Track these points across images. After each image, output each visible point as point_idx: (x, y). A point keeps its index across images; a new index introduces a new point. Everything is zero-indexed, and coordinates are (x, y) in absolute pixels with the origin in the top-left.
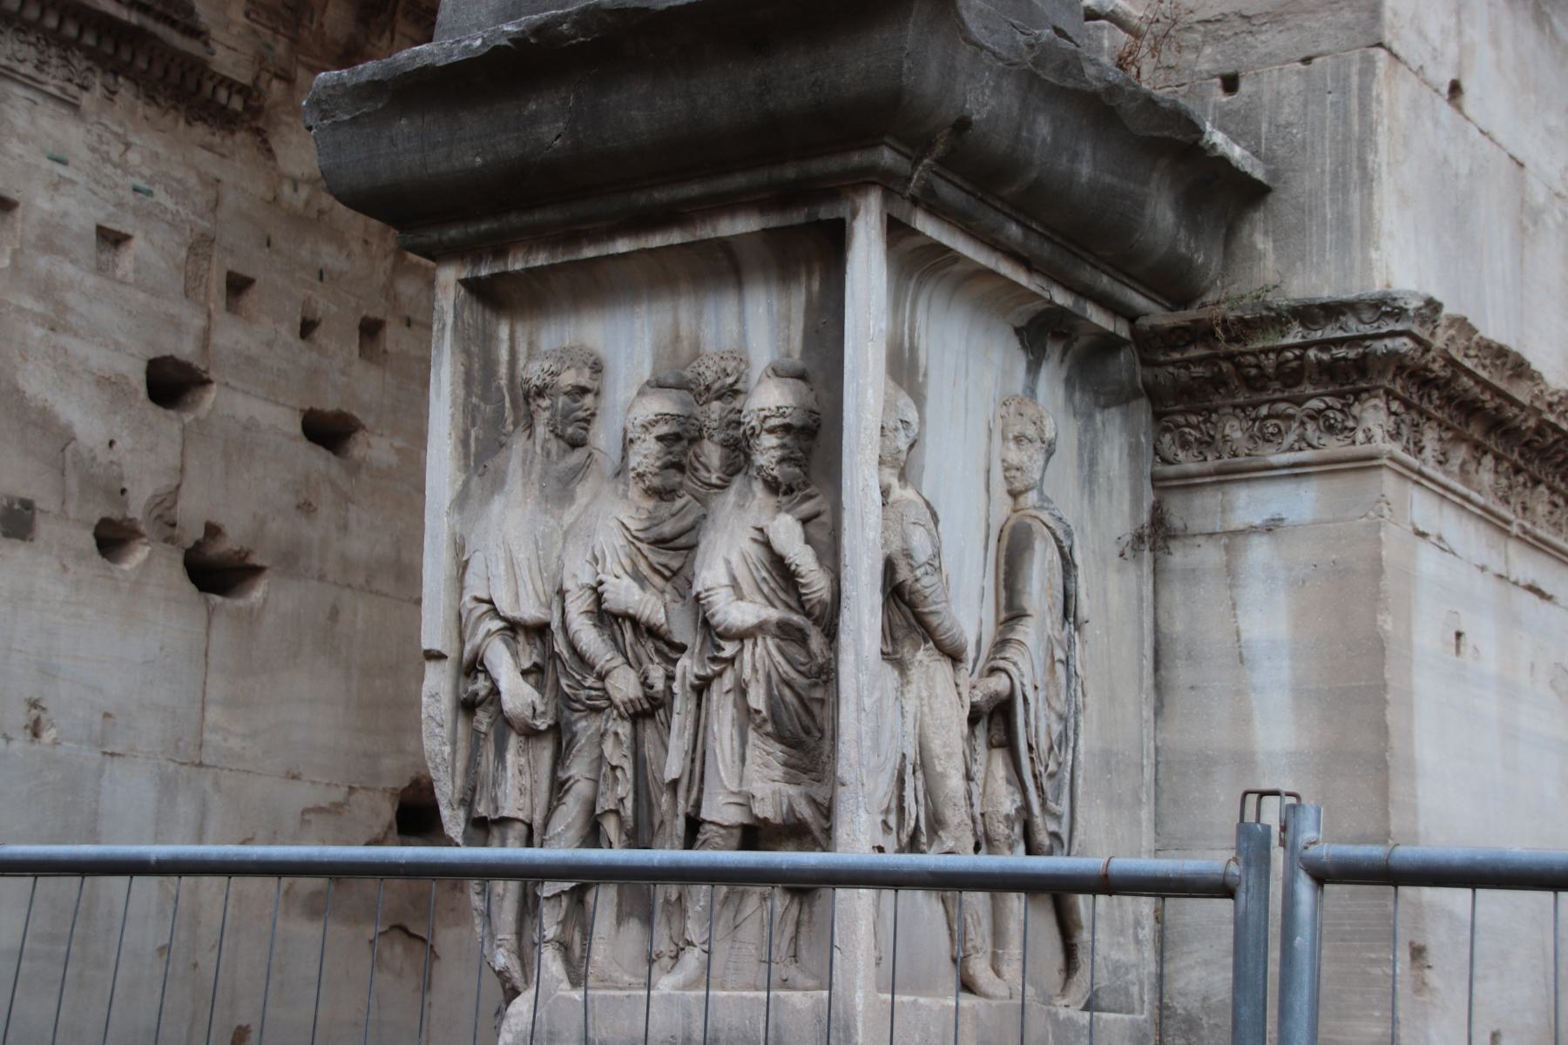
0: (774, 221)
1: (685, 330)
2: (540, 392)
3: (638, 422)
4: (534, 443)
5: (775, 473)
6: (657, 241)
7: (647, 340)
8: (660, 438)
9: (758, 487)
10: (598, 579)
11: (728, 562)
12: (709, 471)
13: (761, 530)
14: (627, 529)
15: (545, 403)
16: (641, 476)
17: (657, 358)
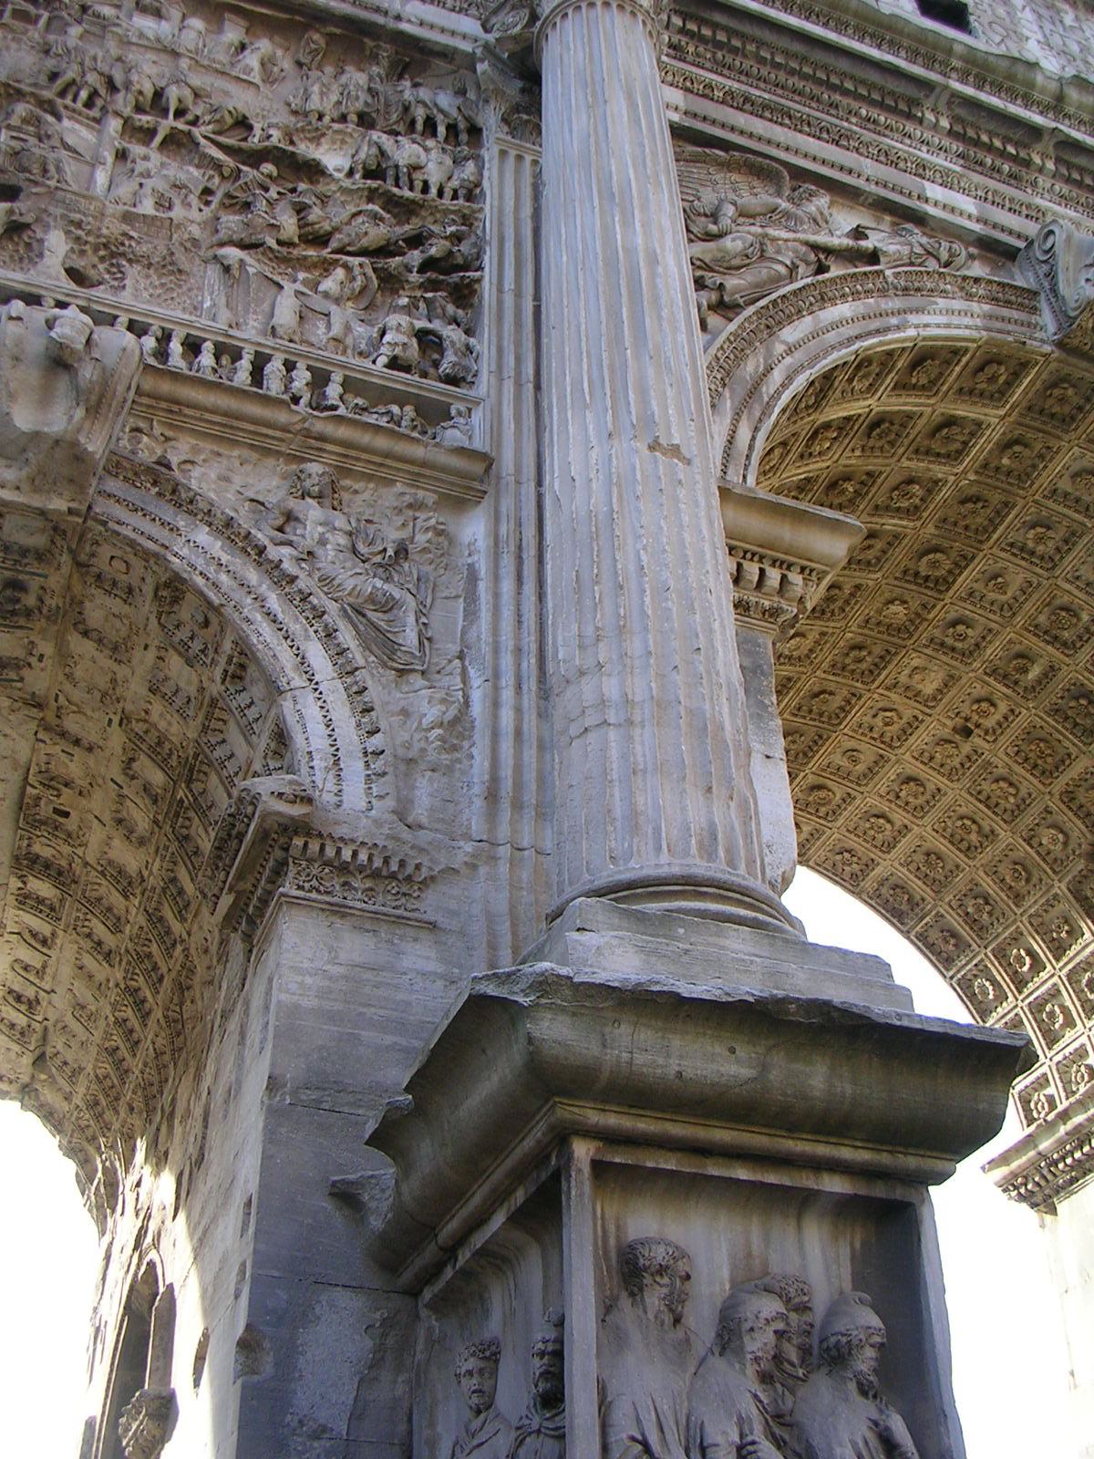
0: (860, 1189)
1: (756, 1250)
2: (662, 1270)
3: (764, 1315)
4: (645, 1312)
5: (871, 1378)
6: (771, 1178)
7: (724, 1250)
8: (776, 1332)
9: (852, 1386)
10: (749, 1438)
11: (854, 1444)
12: (792, 1364)
13: (876, 1423)
14: (761, 1402)
15: (666, 1280)
16: (757, 1360)
17: (734, 1268)
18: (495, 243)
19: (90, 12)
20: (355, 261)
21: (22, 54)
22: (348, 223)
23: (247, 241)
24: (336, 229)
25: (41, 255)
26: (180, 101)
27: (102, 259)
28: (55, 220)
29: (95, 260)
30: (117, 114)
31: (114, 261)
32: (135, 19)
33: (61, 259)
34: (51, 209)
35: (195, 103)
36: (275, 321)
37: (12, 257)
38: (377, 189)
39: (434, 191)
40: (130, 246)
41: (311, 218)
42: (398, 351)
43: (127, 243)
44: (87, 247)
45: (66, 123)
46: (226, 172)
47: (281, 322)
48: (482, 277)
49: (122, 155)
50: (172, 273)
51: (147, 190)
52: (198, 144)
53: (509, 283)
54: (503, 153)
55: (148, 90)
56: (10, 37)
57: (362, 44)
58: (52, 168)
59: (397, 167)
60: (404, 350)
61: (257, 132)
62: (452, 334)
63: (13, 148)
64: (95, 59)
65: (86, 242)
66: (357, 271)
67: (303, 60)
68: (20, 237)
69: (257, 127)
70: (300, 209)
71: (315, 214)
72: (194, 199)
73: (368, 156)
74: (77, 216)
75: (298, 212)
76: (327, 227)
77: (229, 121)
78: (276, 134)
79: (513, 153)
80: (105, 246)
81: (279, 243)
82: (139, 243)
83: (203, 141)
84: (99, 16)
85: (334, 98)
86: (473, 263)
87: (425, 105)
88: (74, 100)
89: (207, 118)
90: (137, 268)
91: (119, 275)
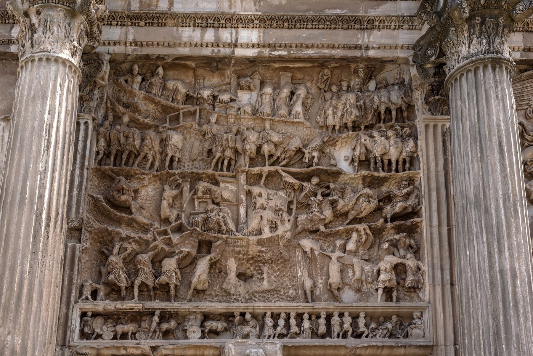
18: (427, 196)
19: (218, 101)
20: (361, 227)
21: (193, 139)
22: (356, 203)
23: (312, 230)
24: (352, 209)
25: (226, 273)
26: (270, 152)
27: (251, 264)
28: (229, 254)
29: (249, 265)
30: (243, 171)
31: (257, 264)
32: (239, 95)
33: (235, 273)
34: (227, 248)
35: (276, 150)
36: (331, 281)
37: (214, 276)
38: (367, 176)
39: (394, 165)
40: (263, 256)
41: (339, 207)
42: (387, 284)
43: (261, 255)
44: (244, 261)
45: (222, 185)
46: (296, 188)
47: (334, 281)
48: (422, 221)
49: (249, 193)
50: (282, 262)
51: (265, 222)
52: (281, 175)
53: (435, 223)
54: (427, 126)
55: (254, 148)
56: (185, 132)
57: (350, 68)
58: (222, 224)
59: (375, 157)
60: (389, 283)
61: (307, 155)
62: (411, 262)
63: (203, 218)
64: (227, 140)
65: (244, 259)
66: (363, 233)
67: (322, 86)
68: (215, 265)
69: (306, 151)
70: (333, 203)
71: (341, 203)
72: (285, 216)
73: (360, 153)
74: (237, 249)
75: (332, 204)
76: (346, 209)
77: (293, 154)
78: (315, 154)
79: (432, 124)
80: (252, 258)
81: (326, 226)
82: (266, 253)
83: (284, 174)
84: (222, 102)
85: (339, 114)
86: (415, 213)
87: (385, 103)
88: (222, 170)
89: (283, 156)
90: (267, 265)
91: (260, 272)
